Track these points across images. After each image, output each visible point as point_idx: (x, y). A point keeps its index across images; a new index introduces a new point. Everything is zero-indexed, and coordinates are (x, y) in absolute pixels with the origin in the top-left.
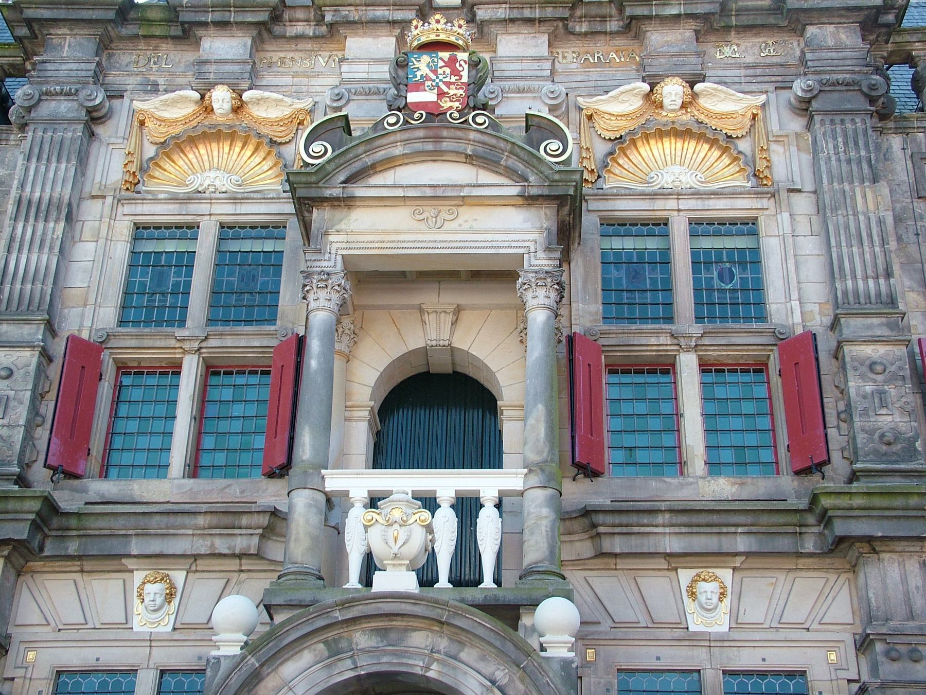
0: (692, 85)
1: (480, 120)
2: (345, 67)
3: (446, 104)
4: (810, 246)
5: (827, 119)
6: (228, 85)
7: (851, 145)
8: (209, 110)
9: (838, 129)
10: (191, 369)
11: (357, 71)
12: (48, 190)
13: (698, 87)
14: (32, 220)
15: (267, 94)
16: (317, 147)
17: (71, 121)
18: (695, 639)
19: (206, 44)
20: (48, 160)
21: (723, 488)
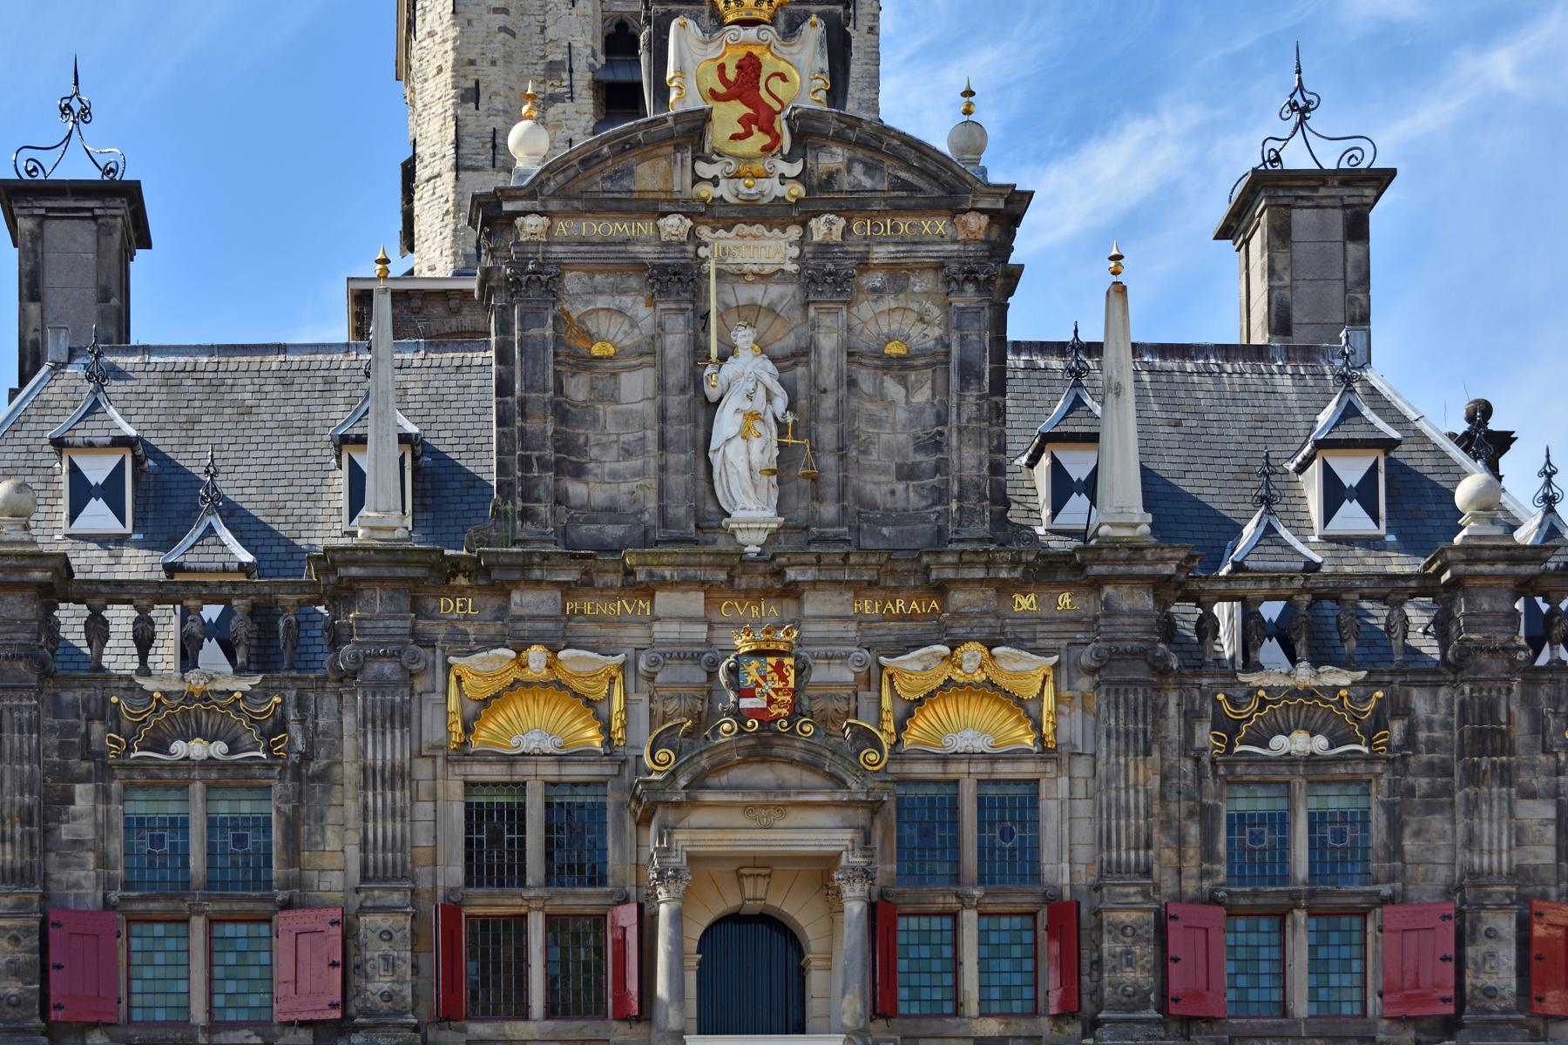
0: (990, 649)
1: (806, 728)
2: (657, 627)
3: (774, 710)
5: (1113, 688)
6: (546, 646)
7: (1132, 716)
8: (524, 666)
9: (1122, 699)
11: (666, 631)
12: (389, 757)
13: (995, 651)
14: (379, 790)
15: (582, 653)
16: (661, 755)
17: (396, 684)
19: (516, 597)
20: (383, 726)
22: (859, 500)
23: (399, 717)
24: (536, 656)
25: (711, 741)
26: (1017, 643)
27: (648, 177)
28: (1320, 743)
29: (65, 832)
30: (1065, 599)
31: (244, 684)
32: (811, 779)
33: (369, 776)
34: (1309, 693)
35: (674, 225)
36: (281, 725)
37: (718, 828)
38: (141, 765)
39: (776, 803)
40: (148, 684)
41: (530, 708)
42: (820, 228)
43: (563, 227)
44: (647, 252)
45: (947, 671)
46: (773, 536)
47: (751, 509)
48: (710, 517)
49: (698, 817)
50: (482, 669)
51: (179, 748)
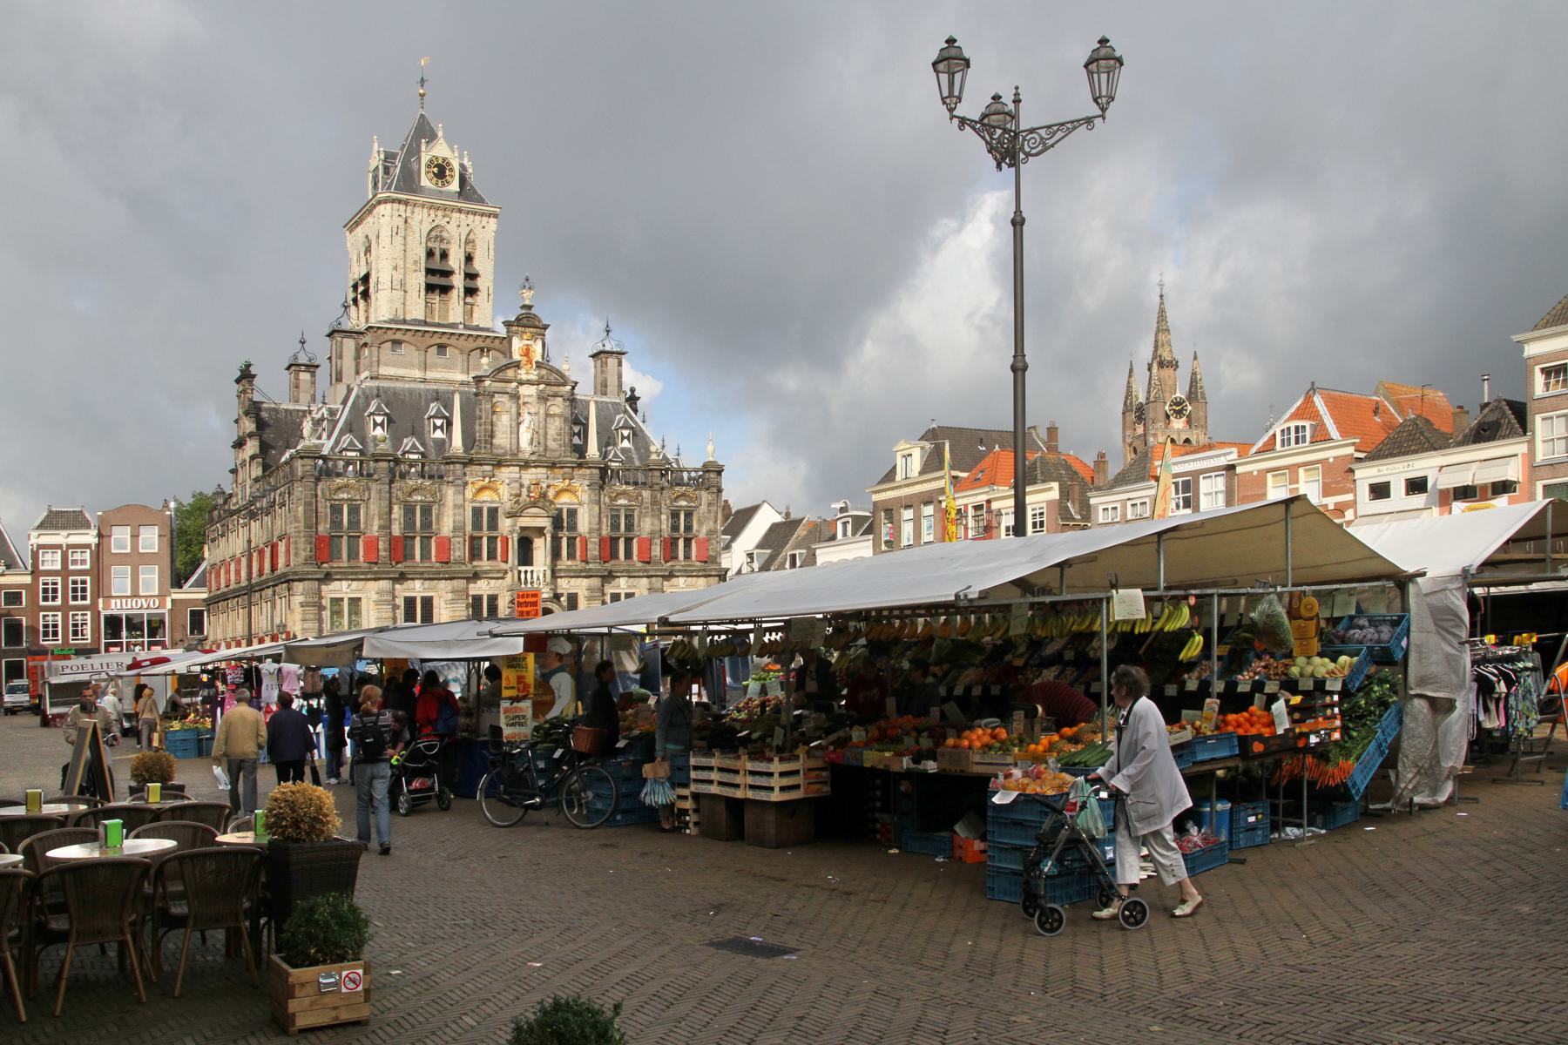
10: (485, 540)
27: (510, 373)
33: (455, 506)
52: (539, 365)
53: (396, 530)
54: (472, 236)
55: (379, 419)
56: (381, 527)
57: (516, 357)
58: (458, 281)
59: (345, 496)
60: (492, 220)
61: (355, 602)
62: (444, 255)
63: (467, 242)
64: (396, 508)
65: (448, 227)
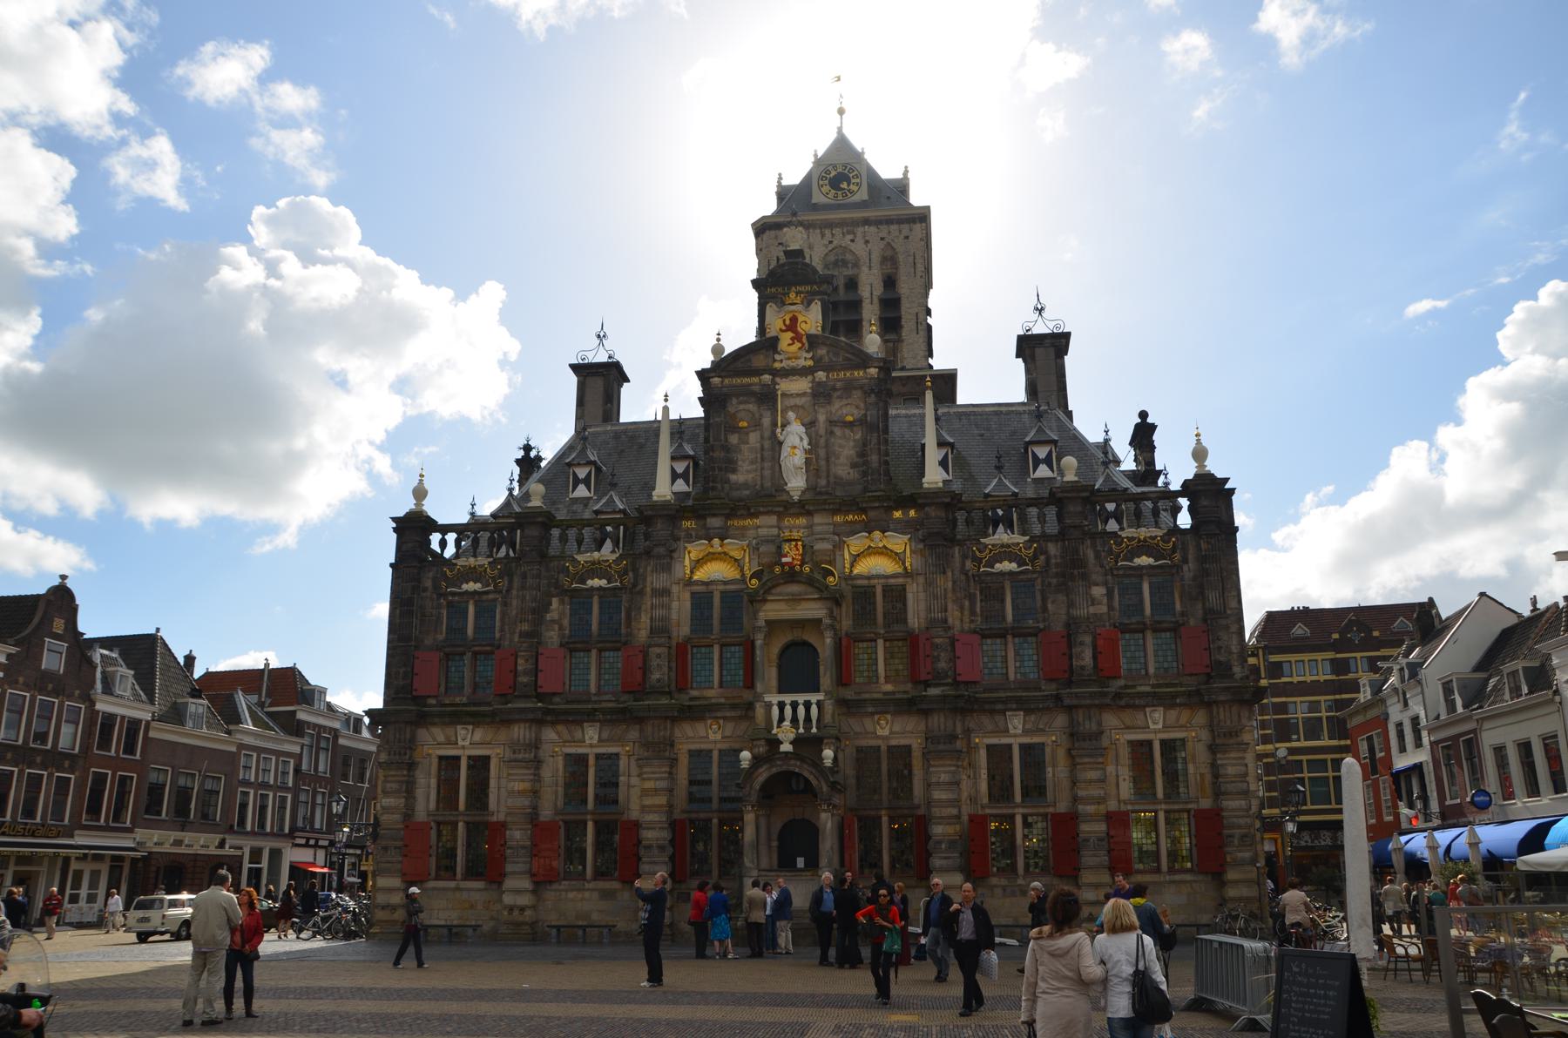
4: (922, 596)
10: (716, 649)
11: (763, 532)
18: (878, 737)
21: (889, 688)
22: (836, 477)
23: (668, 568)
24: (716, 541)
25: (774, 576)
26: (895, 531)
27: (759, 361)
28: (1013, 566)
29: (548, 616)
30: (912, 513)
31: (614, 557)
32: (810, 589)
34: (1008, 546)
35: (767, 378)
36: (626, 573)
37: (774, 610)
38: (575, 590)
39: (795, 600)
40: (579, 558)
41: (712, 564)
42: (821, 375)
43: (726, 381)
44: (756, 388)
45: (868, 543)
46: (803, 492)
47: (796, 483)
48: (780, 487)
49: (768, 606)
50: (694, 550)
51: (590, 583)
52: (813, 342)
53: (552, 637)
54: (889, 253)
55: (582, 473)
56: (522, 635)
57: (771, 333)
58: (870, 313)
59: (471, 586)
60: (917, 227)
61: (480, 765)
62: (852, 284)
63: (884, 260)
64: (555, 601)
65: (853, 247)
